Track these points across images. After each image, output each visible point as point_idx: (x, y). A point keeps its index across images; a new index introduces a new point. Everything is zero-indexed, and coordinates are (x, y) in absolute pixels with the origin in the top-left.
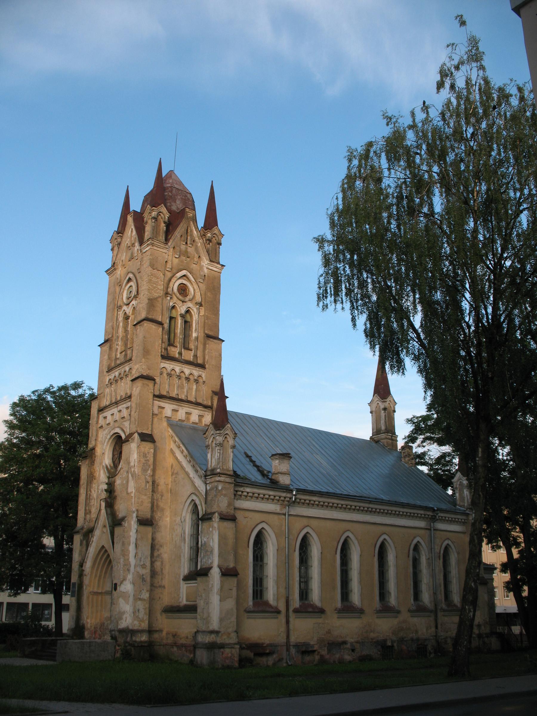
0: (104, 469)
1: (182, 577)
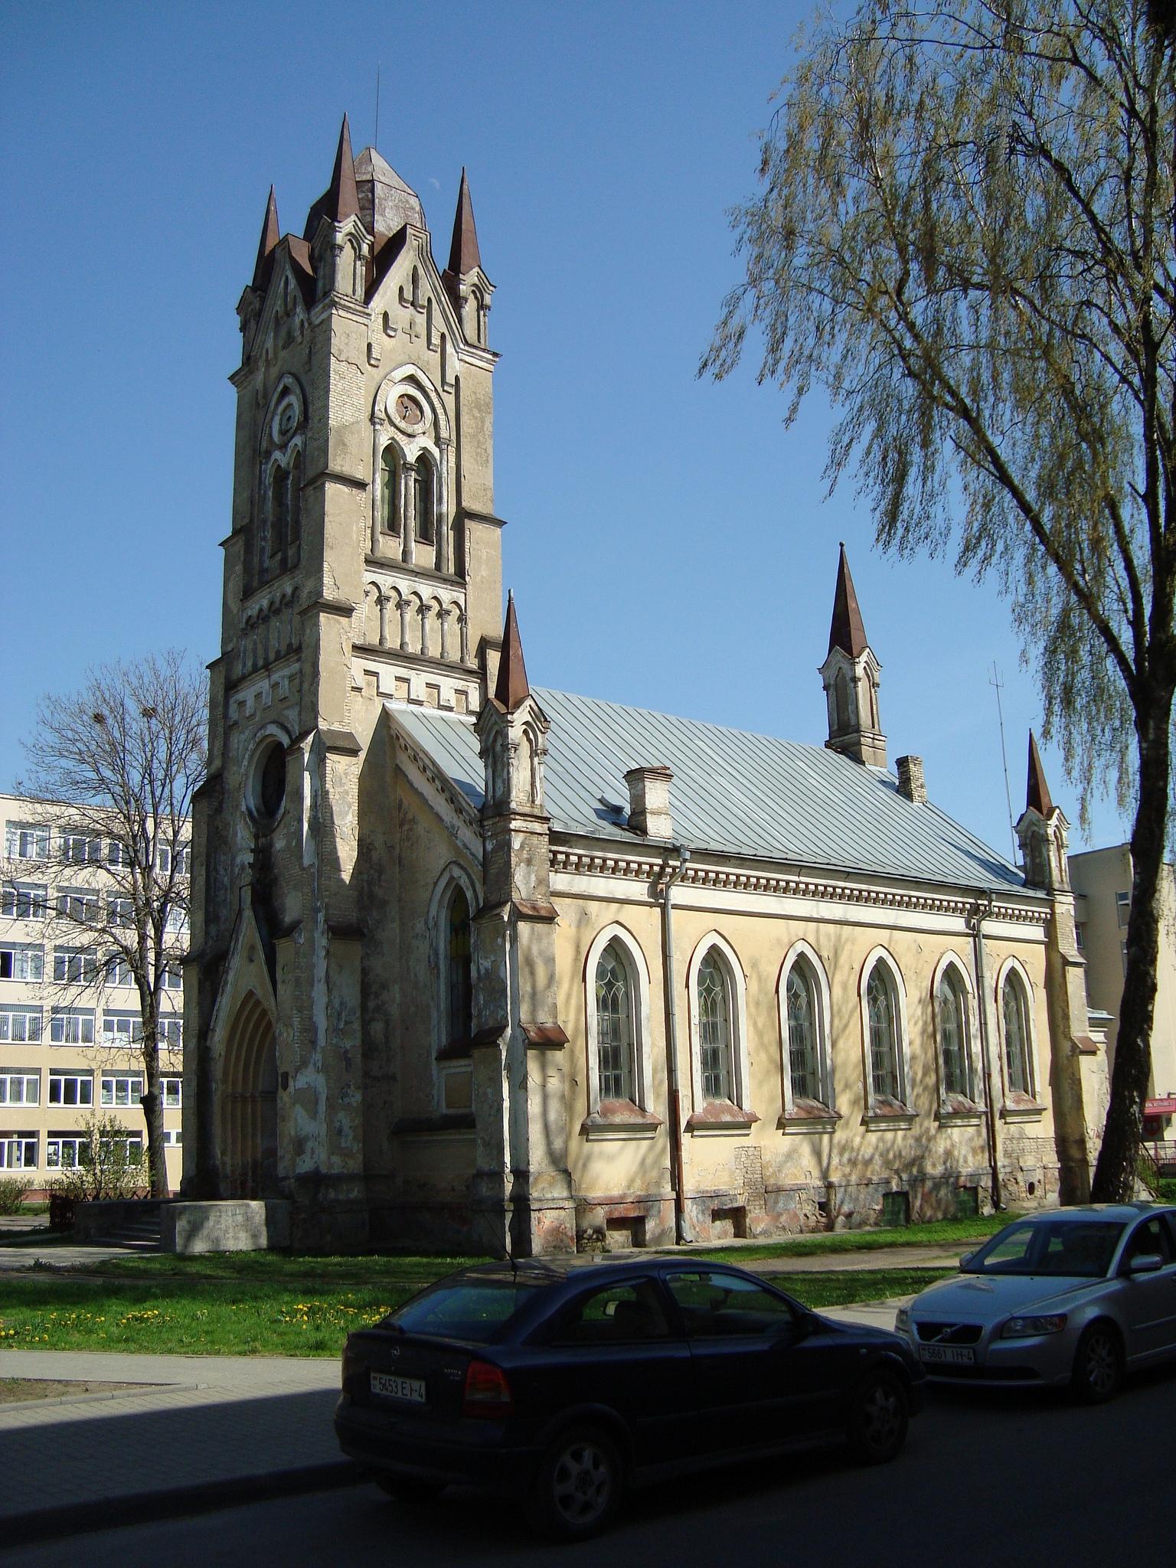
0: (245, 820)
1: (434, 1055)
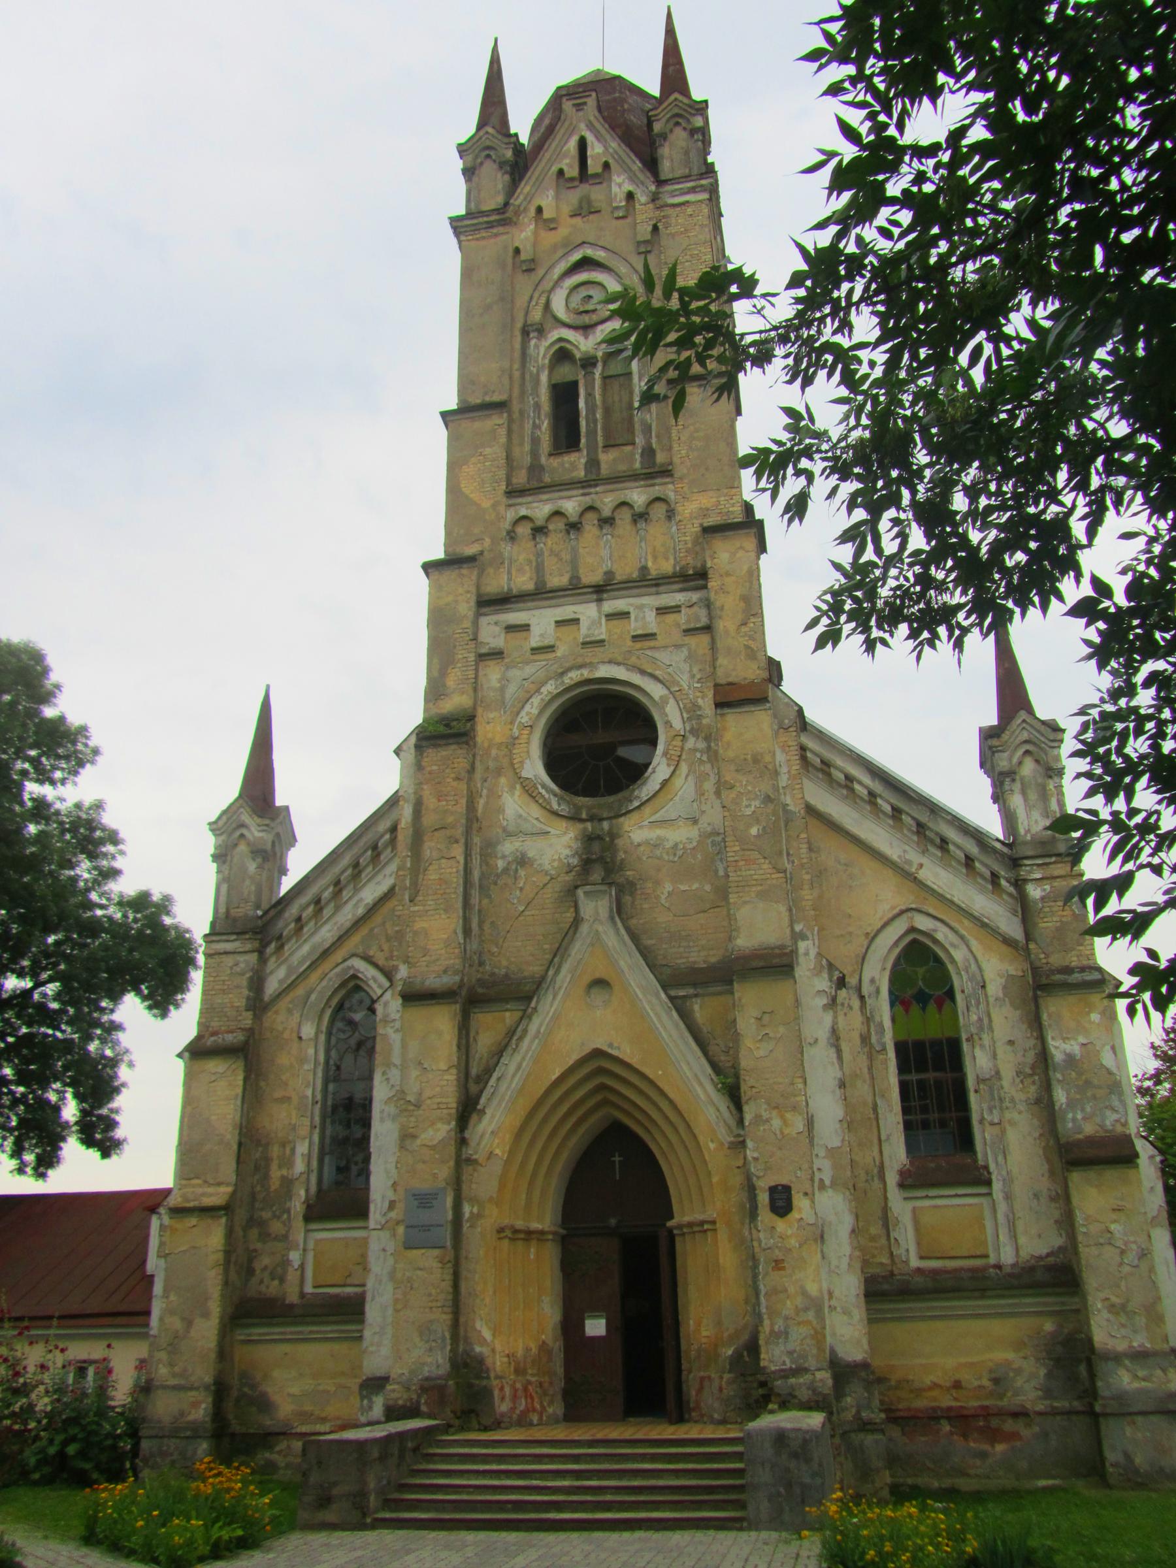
1: (892, 1179)
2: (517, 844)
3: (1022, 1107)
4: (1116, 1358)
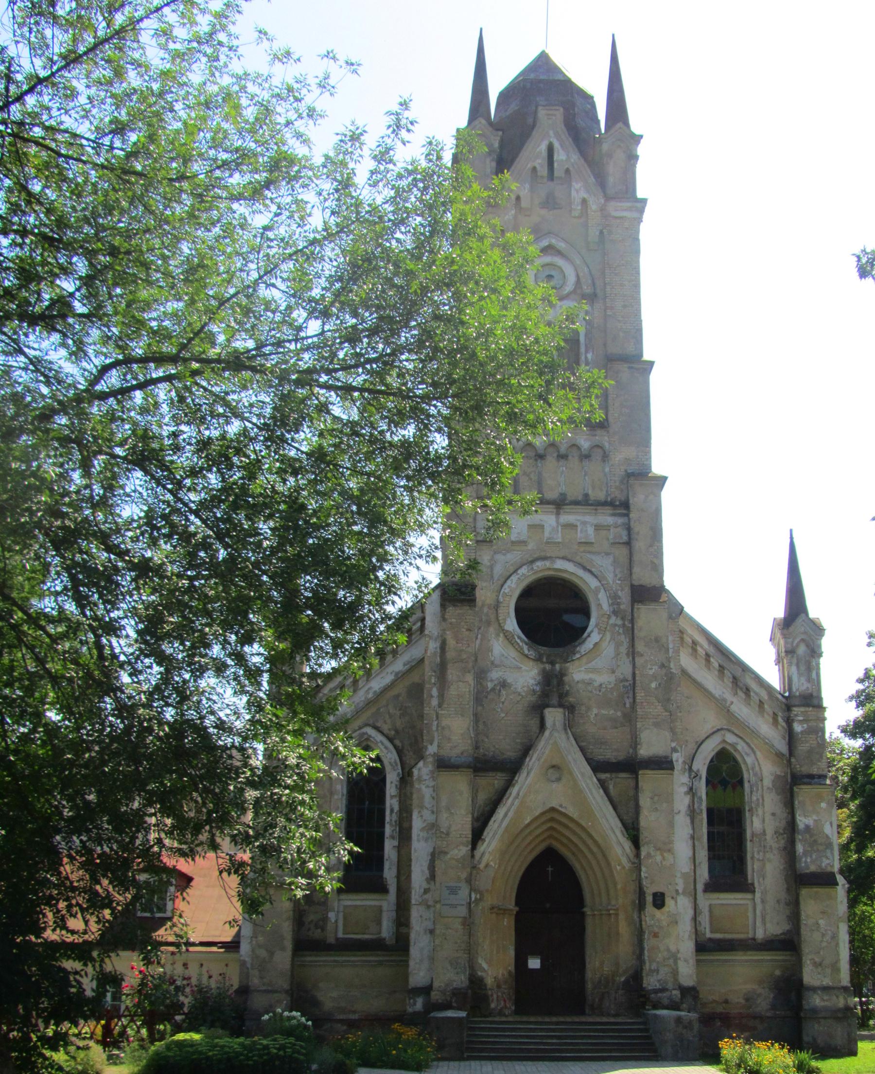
1: (700, 887)
2: (501, 673)
3: (775, 852)
4: (814, 989)
